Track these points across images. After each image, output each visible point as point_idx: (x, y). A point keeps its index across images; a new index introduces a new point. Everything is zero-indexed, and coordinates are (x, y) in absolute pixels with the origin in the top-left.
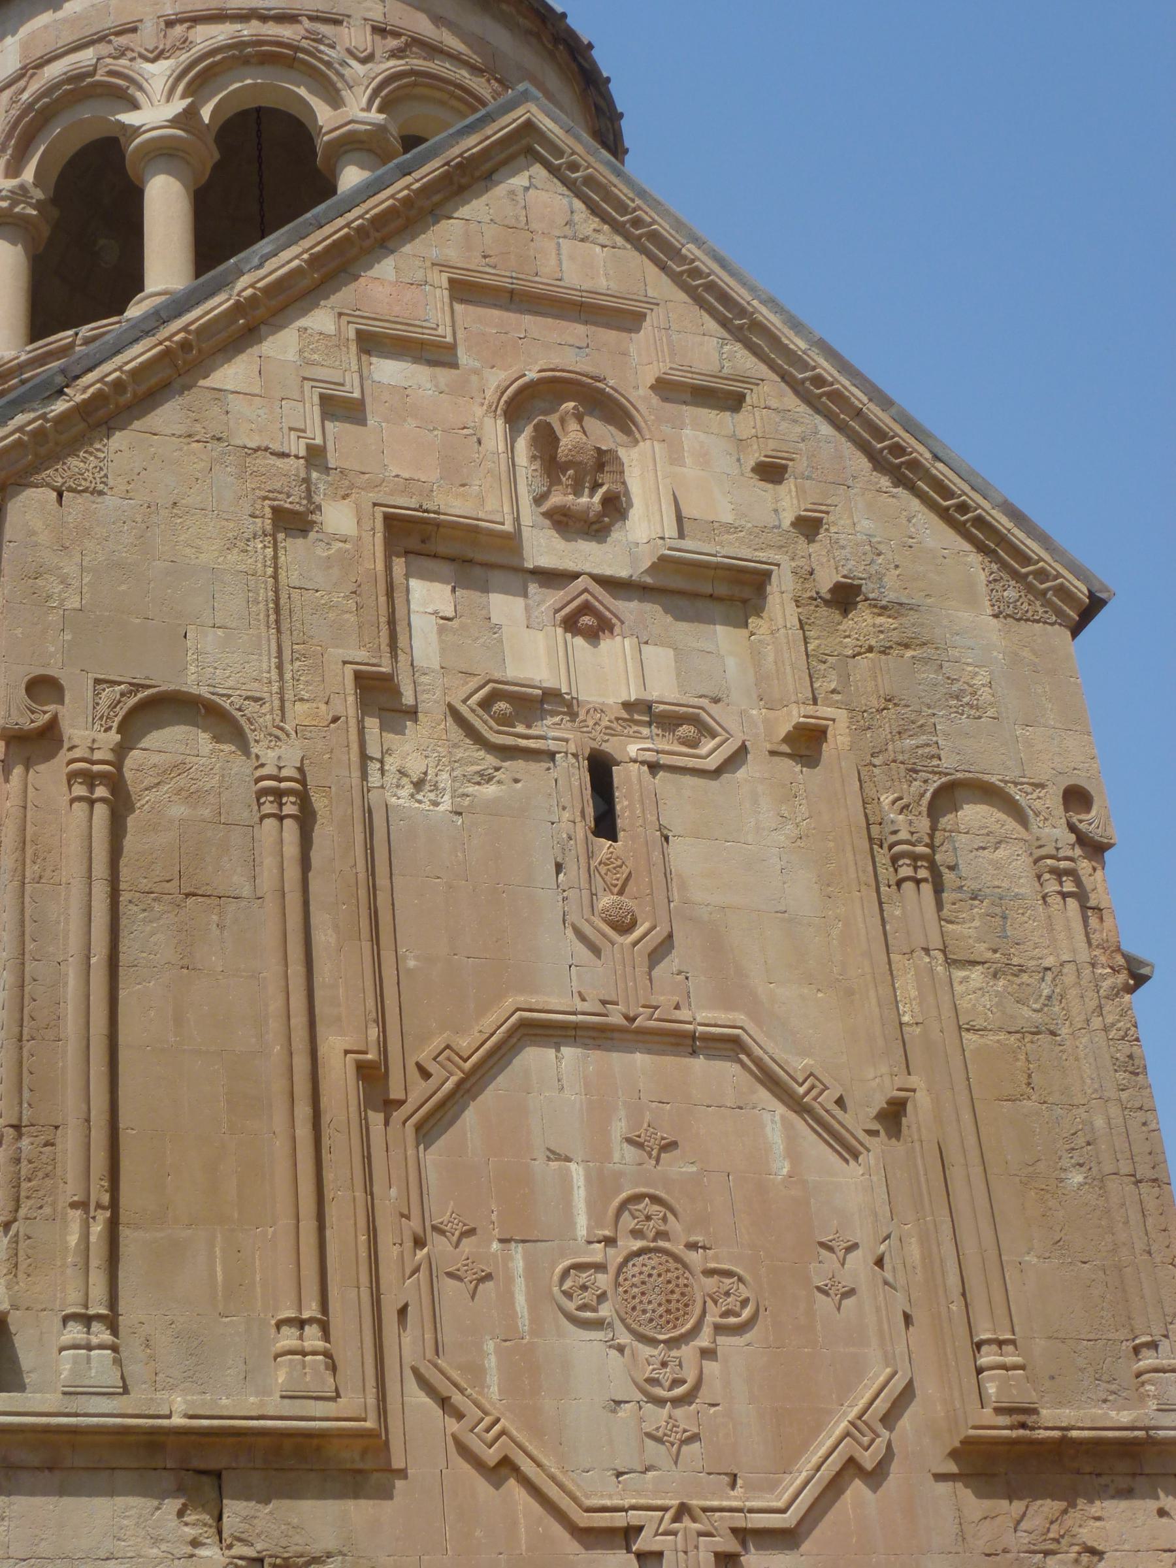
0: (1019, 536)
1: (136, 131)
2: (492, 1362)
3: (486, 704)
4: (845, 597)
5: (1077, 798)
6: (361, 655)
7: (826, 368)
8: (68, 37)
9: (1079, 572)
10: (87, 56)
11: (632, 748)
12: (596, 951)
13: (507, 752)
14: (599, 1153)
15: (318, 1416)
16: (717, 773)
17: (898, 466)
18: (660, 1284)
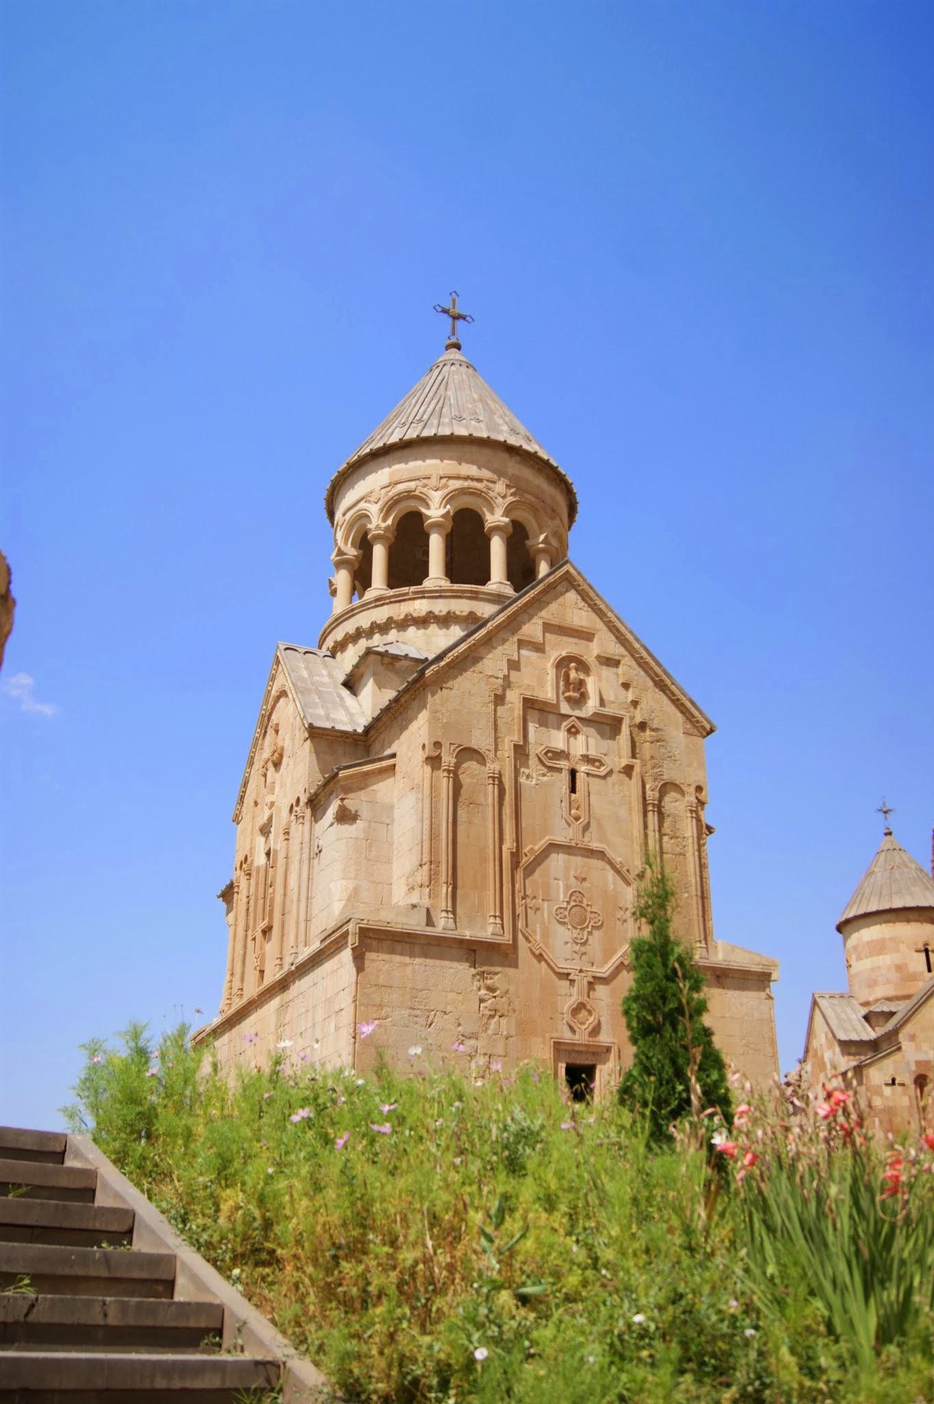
0: (693, 710)
1: (429, 517)
2: (538, 930)
3: (546, 754)
4: (642, 726)
5: (699, 789)
6: (516, 738)
7: (644, 654)
8: (405, 477)
9: (709, 722)
10: (412, 485)
11: (583, 768)
12: (569, 825)
13: (551, 769)
14: (567, 879)
15: (498, 940)
16: (604, 777)
17: (661, 686)
18: (578, 914)
